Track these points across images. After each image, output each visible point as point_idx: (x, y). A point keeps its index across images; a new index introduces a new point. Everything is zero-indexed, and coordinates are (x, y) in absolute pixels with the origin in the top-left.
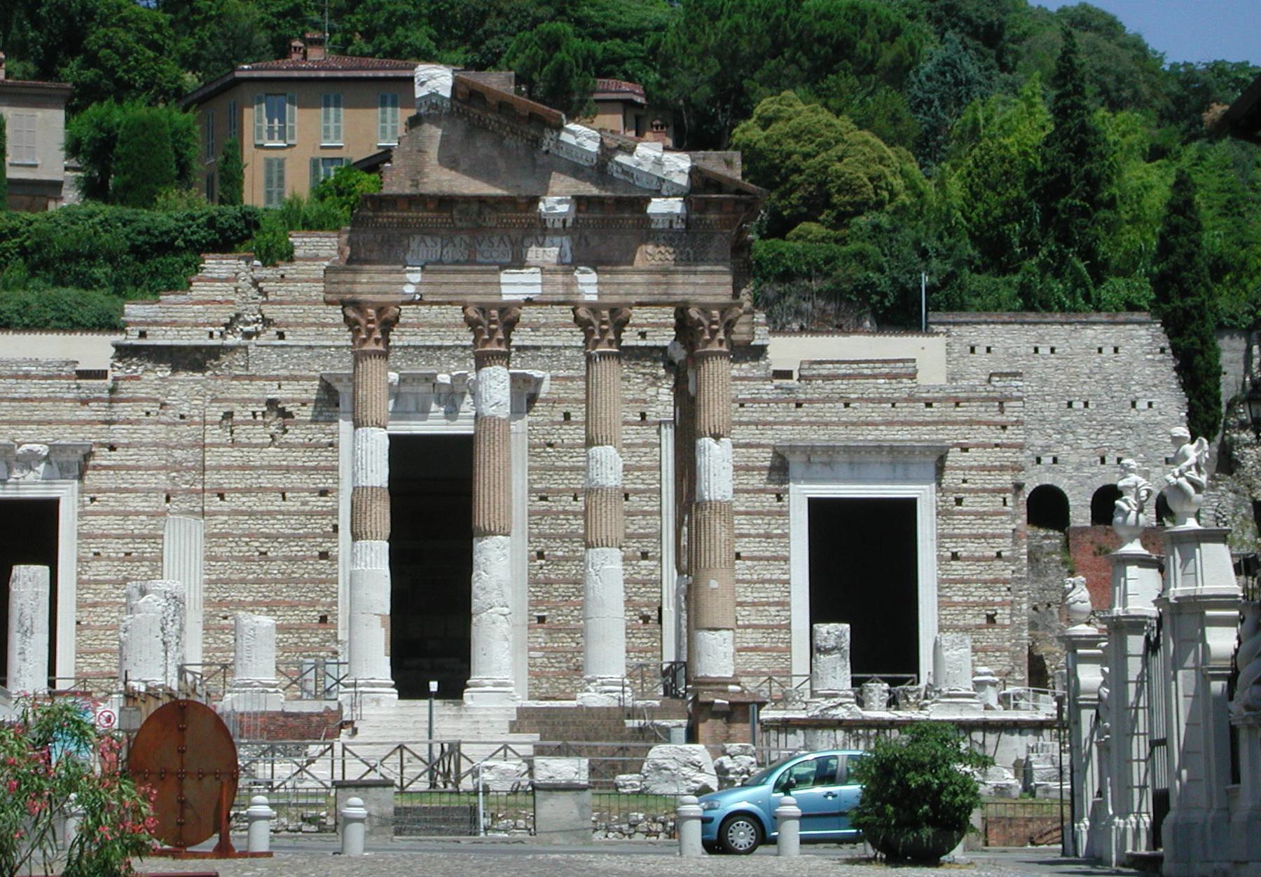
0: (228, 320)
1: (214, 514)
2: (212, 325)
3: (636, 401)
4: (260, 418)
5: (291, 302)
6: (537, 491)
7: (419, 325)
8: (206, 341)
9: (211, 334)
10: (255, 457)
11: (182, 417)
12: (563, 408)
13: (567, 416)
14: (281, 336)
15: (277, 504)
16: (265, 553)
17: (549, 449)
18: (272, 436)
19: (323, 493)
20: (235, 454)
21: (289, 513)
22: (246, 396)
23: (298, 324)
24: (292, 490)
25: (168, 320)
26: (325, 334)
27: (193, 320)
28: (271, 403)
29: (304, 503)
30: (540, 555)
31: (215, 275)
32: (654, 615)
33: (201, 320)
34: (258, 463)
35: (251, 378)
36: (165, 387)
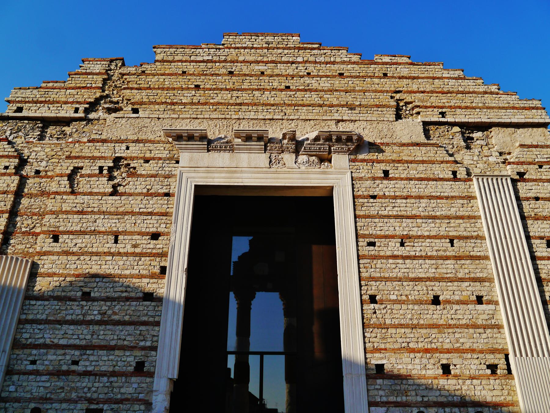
0: (92, 100)
1: (46, 253)
2: (78, 103)
3: (447, 162)
4: (105, 172)
5: (149, 88)
6: (364, 236)
7: (255, 104)
8: (71, 114)
9: (76, 110)
10: (94, 203)
11: (38, 172)
12: (383, 166)
13: (386, 173)
14: (136, 111)
15: (109, 245)
16: (89, 293)
17: (372, 200)
18: (114, 187)
19: (155, 236)
20: (76, 201)
21: (119, 254)
22: (97, 154)
23: (151, 103)
24: (125, 233)
25: (40, 99)
26: (174, 110)
27: (64, 99)
28: (117, 160)
29: (135, 246)
30: (373, 299)
31: (88, 71)
32: (502, 364)
33: (71, 100)
34: (96, 210)
35: (104, 141)
36: (29, 148)
